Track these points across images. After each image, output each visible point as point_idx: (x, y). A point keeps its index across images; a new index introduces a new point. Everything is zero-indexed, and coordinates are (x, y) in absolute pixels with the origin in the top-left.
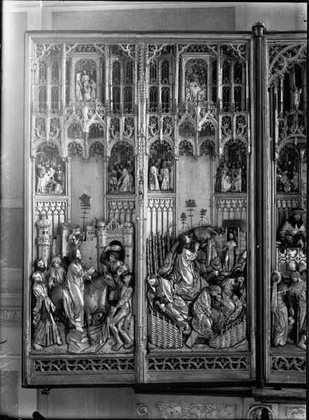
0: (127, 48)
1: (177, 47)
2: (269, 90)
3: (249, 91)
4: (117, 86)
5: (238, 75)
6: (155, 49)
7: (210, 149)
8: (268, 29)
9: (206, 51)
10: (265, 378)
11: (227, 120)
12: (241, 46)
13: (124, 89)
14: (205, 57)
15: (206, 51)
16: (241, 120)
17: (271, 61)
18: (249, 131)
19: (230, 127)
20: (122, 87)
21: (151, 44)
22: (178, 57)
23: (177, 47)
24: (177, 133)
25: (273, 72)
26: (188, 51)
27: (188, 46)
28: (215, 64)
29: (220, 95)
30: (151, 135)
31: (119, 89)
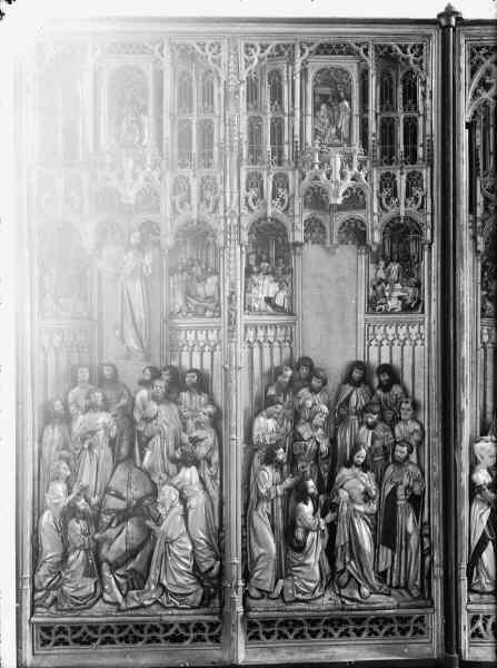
0: (207, 48)
1: (298, 47)
2: (469, 126)
3: (430, 125)
4: (185, 117)
5: (410, 94)
6: (256, 51)
7: (357, 233)
8: (467, 16)
9: (350, 54)
10: (459, 652)
11: (388, 182)
12: (414, 47)
13: (199, 123)
14: (350, 66)
15: (350, 52)
16: (414, 180)
17: (473, 72)
18: (429, 200)
19: (395, 193)
20: (194, 120)
21: (250, 42)
22: (298, 66)
23: (298, 47)
24: (298, 202)
25: (475, 94)
26: (318, 53)
27: (315, 46)
28: (364, 75)
29: (373, 128)
30: (249, 207)
31: (190, 122)
